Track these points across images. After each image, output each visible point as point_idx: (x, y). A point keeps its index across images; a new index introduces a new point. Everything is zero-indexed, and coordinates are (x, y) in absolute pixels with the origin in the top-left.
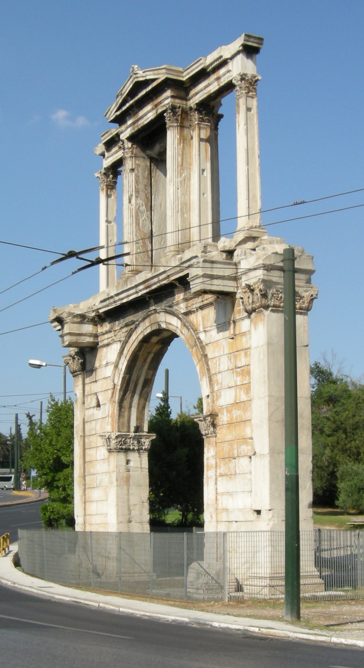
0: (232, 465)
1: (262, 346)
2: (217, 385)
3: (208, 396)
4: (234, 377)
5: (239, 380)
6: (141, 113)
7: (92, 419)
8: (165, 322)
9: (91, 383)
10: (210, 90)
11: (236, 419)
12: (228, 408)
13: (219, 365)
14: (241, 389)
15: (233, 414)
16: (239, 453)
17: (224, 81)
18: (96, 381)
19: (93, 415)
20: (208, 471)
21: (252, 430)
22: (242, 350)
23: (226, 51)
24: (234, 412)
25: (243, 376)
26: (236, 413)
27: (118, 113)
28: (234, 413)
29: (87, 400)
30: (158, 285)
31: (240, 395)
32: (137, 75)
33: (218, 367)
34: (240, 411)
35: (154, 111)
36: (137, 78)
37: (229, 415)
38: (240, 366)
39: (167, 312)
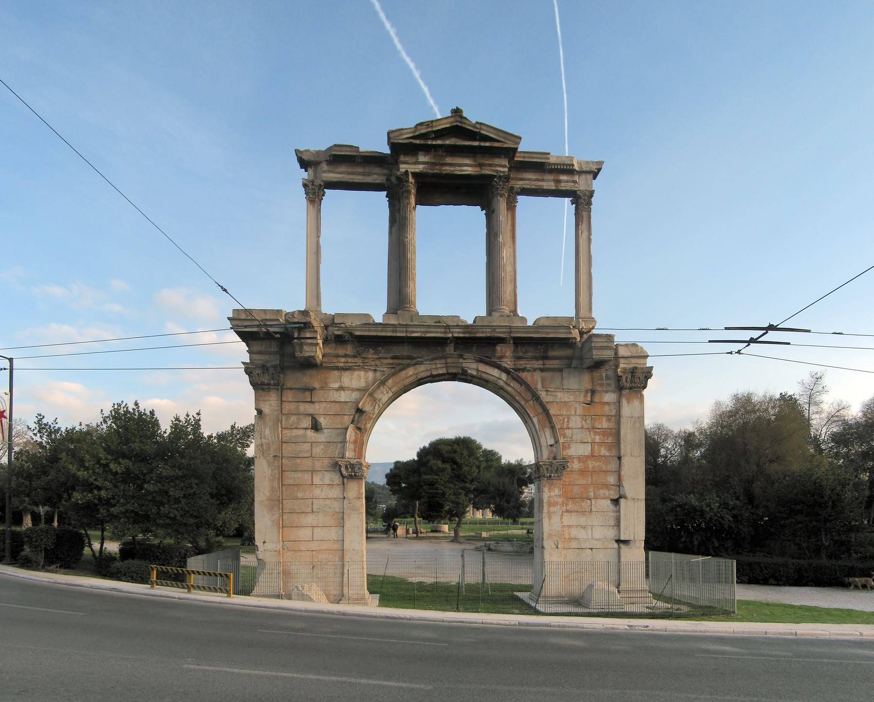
1: (638, 417)
3: (551, 446)
4: (590, 435)
5: (597, 439)
6: (449, 160)
8: (477, 370)
9: (298, 402)
10: (543, 186)
11: (593, 468)
13: (568, 422)
14: (601, 446)
15: (588, 464)
17: (564, 186)
18: (311, 402)
19: (305, 436)
21: (619, 479)
22: (603, 416)
26: (591, 464)
27: (418, 142)
28: (590, 464)
29: (287, 420)
31: (599, 450)
32: (464, 121)
33: (565, 424)
34: (598, 463)
35: (477, 169)
36: (461, 122)
37: (581, 464)
38: (600, 427)
39: (481, 361)
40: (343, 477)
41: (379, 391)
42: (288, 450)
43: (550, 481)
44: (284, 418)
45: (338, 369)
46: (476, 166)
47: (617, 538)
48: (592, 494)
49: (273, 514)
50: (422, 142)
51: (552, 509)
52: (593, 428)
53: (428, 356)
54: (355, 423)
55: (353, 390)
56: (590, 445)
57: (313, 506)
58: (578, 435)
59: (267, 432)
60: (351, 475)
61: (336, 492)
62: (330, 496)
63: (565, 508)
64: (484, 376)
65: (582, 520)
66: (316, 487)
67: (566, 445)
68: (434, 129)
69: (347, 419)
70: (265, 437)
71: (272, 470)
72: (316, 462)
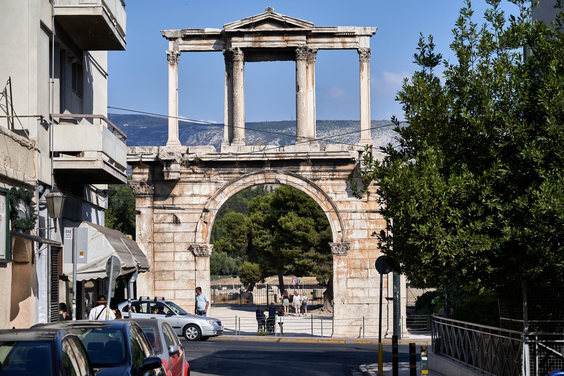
0: (364, 272)
2: (348, 226)
3: (339, 232)
6: (265, 38)
7: (166, 230)
8: (287, 180)
11: (369, 247)
12: (361, 241)
16: (371, 266)
17: (348, 46)
19: (169, 228)
20: (338, 274)
23: (358, 30)
24: (367, 243)
25: (376, 224)
30: (293, 158)
33: (349, 216)
35: (285, 43)
37: (361, 244)
40: (195, 256)
41: (219, 197)
42: (158, 238)
43: (338, 257)
44: (155, 216)
45: (190, 182)
46: (284, 41)
47: (386, 296)
48: (368, 266)
49: (148, 282)
50: (246, 30)
51: (340, 276)
52: (369, 219)
53: (252, 172)
54: (203, 218)
55: (200, 196)
56: (367, 231)
57: (175, 275)
58: (358, 224)
59: (144, 226)
60: (201, 255)
61: (192, 266)
62: (186, 268)
63: (349, 276)
64: (291, 184)
65: (362, 284)
66: (177, 263)
67: (350, 231)
68: (254, 21)
69: (197, 216)
70: (143, 230)
71: (148, 251)
72: (177, 246)
